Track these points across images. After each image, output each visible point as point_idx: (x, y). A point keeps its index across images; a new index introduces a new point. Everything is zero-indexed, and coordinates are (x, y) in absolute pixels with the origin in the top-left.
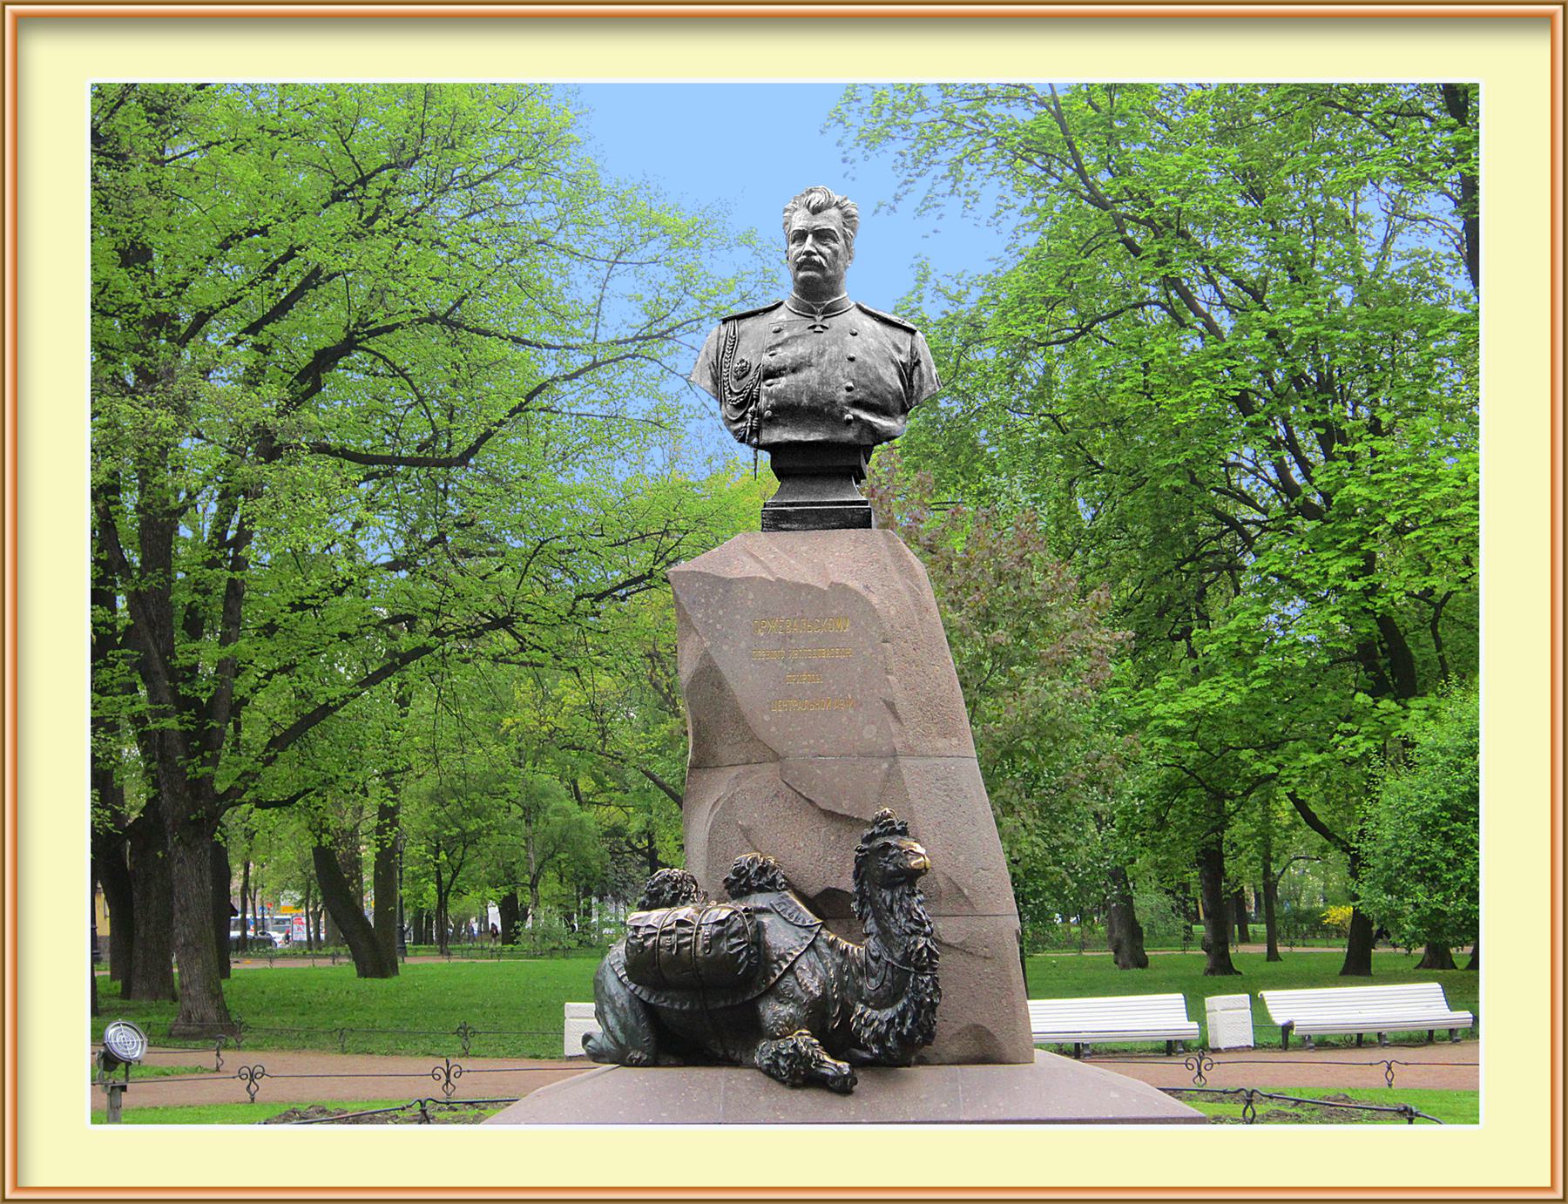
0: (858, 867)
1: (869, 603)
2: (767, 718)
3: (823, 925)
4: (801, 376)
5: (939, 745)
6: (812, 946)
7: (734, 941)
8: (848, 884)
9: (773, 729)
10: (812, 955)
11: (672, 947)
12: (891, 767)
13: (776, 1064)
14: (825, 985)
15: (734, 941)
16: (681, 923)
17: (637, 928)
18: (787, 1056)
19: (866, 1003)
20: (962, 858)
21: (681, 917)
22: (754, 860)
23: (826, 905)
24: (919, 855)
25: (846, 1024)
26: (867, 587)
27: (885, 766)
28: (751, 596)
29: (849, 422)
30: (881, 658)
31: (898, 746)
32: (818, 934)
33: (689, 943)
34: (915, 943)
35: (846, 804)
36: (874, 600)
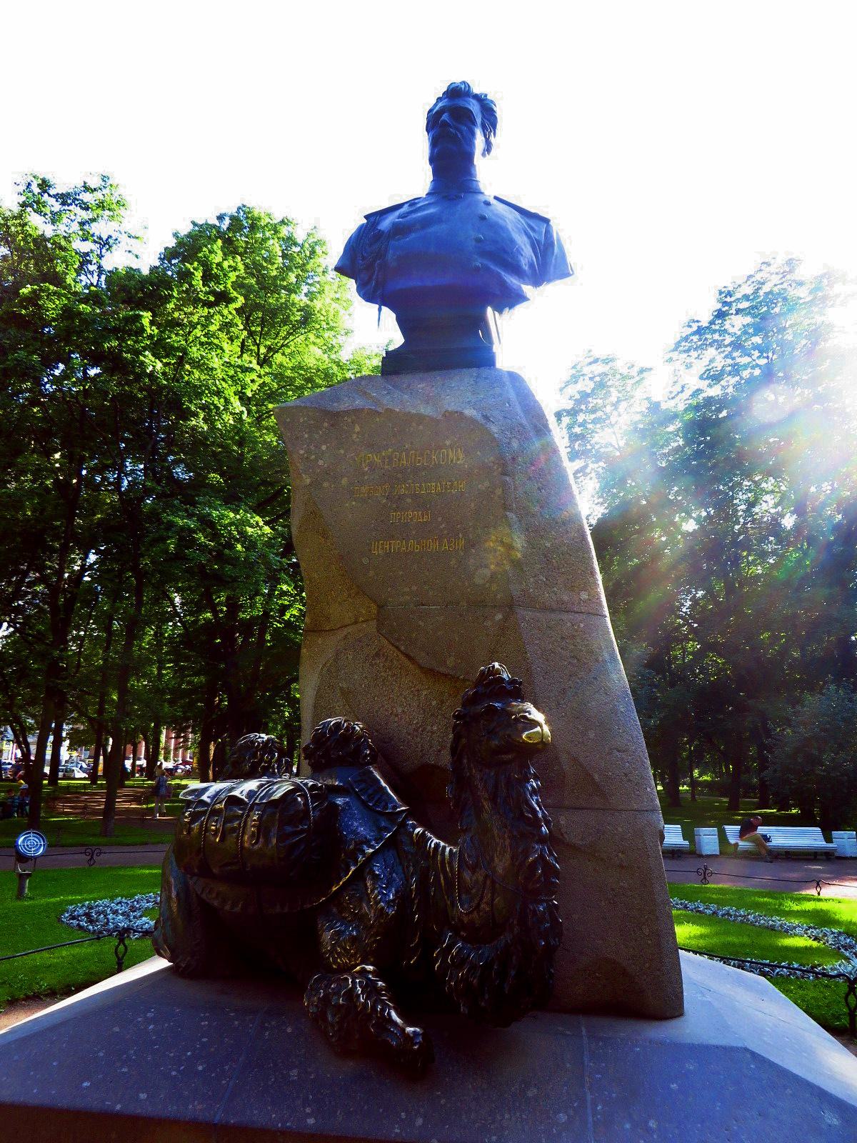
0: (457, 738)
1: (489, 433)
2: (365, 561)
3: (409, 814)
4: (433, 229)
5: (566, 598)
6: (391, 844)
7: (289, 829)
8: (446, 759)
9: (371, 573)
10: (390, 856)
11: (216, 831)
12: (506, 619)
13: (323, 1015)
14: (403, 899)
15: (289, 829)
16: (234, 801)
17: (189, 803)
18: (339, 1007)
19: (456, 931)
20: (592, 735)
21: (236, 793)
22: (338, 725)
23: (419, 786)
24: (535, 723)
25: (427, 960)
26: (486, 418)
27: (499, 617)
28: (357, 429)
29: (477, 269)
30: (499, 491)
31: (516, 593)
32: (403, 825)
33: (234, 830)
34: (526, 854)
35: (450, 662)
36: (494, 429)
